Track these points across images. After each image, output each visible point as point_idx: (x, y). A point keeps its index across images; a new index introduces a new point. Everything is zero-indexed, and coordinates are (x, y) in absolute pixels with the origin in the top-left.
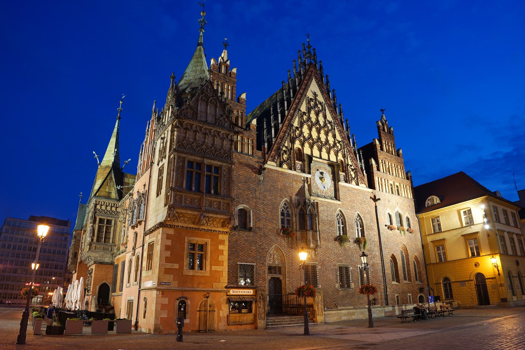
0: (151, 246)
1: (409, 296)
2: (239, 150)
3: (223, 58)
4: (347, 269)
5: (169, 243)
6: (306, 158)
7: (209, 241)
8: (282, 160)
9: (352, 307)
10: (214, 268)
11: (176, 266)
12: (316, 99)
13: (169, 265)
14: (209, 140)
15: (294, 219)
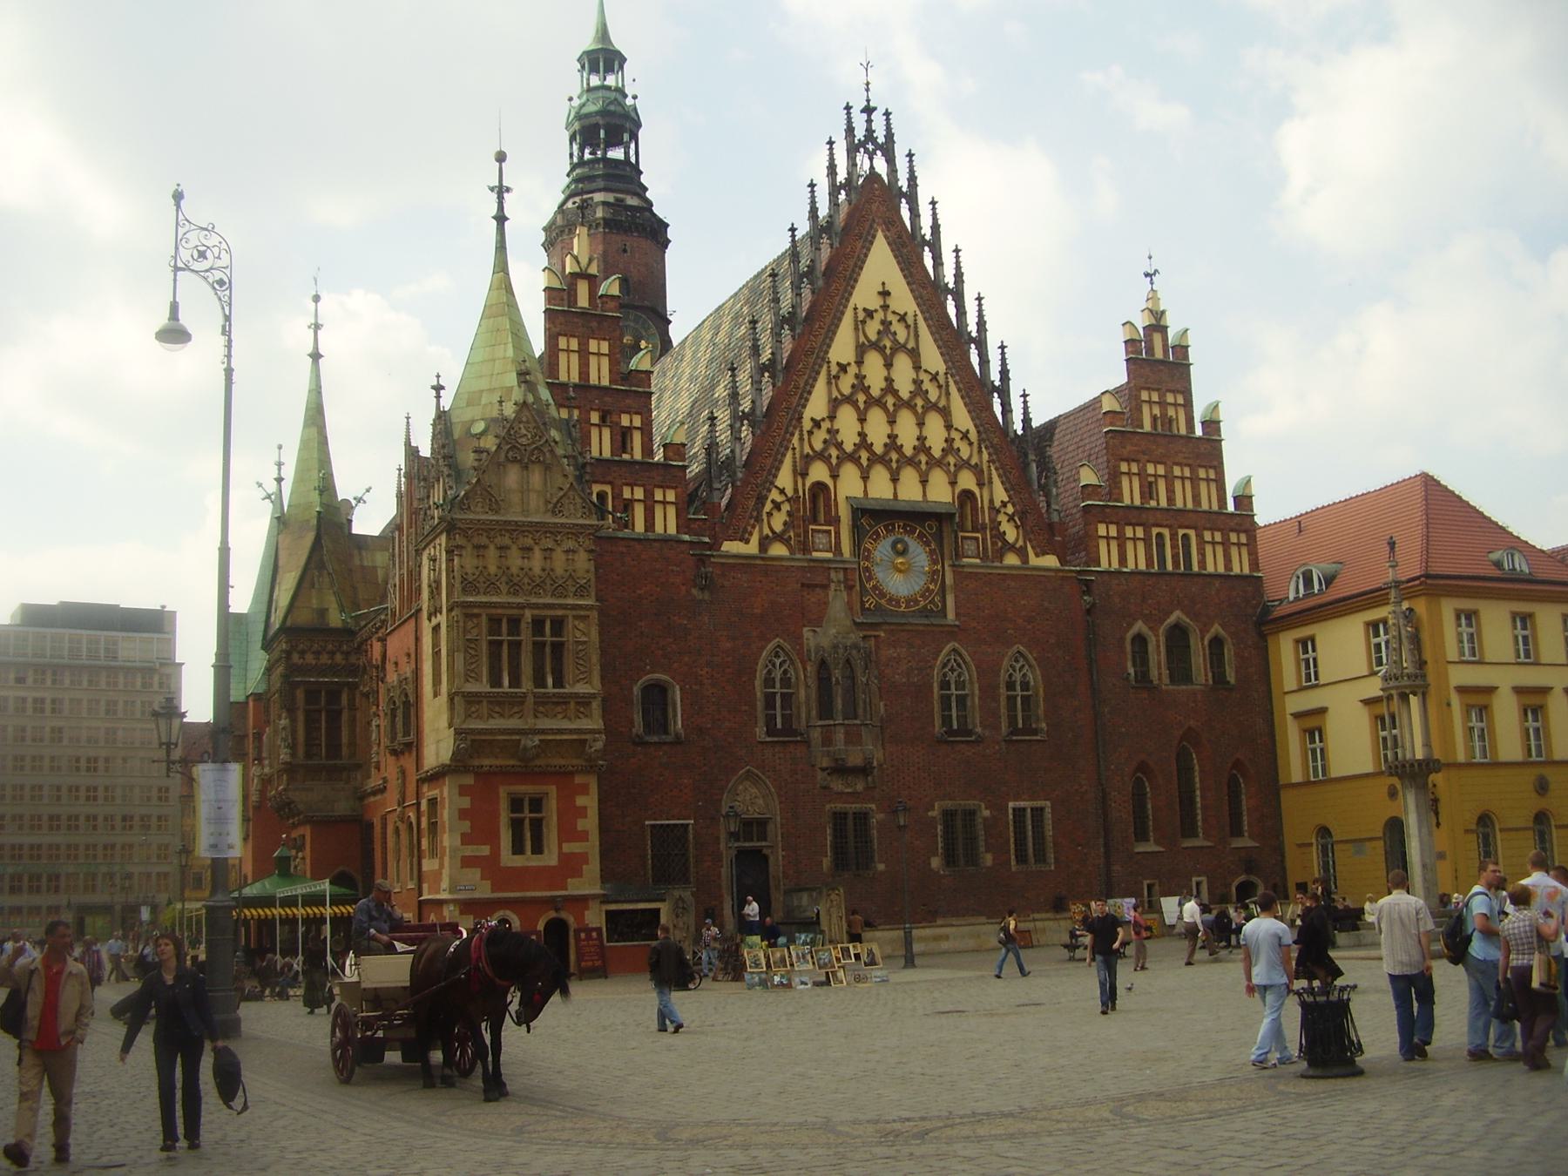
0: (433, 802)
1: (1198, 884)
2: (640, 526)
3: (576, 258)
4: (971, 814)
5: (466, 802)
6: (844, 513)
7: (552, 790)
8: (766, 531)
9: (983, 919)
10: (568, 848)
11: (485, 850)
12: (885, 307)
13: (470, 851)
14: (537, 562)
15: (802, 693)
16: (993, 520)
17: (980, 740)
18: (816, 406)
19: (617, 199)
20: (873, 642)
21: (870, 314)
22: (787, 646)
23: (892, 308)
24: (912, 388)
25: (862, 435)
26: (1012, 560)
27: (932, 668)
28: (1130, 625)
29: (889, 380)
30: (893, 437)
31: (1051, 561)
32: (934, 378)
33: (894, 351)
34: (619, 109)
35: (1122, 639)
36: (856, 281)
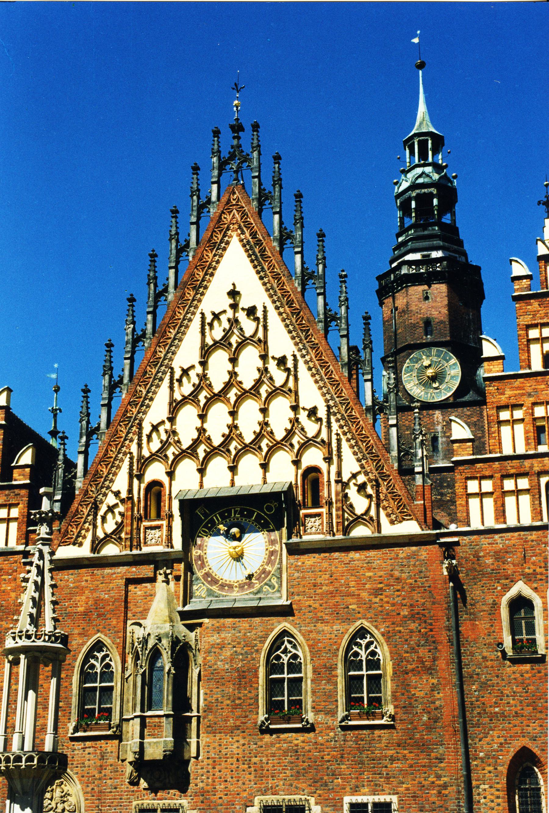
8: (100, 534)
16: (337, 494)
17: (311, 729)
18: (158, 410)
19: (423, 256)
20: (198, 630)
21: (216, 316)
22: (107, 641)
23: (241, 306)
24: (257, 376)
25: (201, 431)
26: (361, 531)
27: (258, 651)
28: (506, 588)
29: (233, 374)
30: (233, 427)
31: (411, 527)
32: (282, 361)
33: (241, 345)
34: (427, 180)
35: (496, 605)
36: (206, 288)
